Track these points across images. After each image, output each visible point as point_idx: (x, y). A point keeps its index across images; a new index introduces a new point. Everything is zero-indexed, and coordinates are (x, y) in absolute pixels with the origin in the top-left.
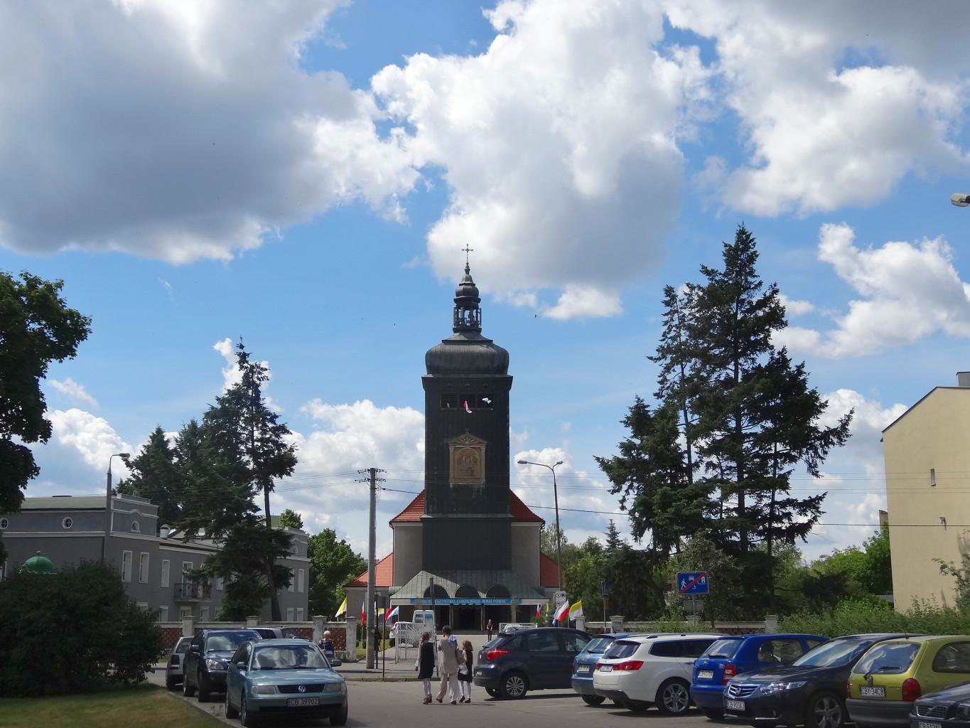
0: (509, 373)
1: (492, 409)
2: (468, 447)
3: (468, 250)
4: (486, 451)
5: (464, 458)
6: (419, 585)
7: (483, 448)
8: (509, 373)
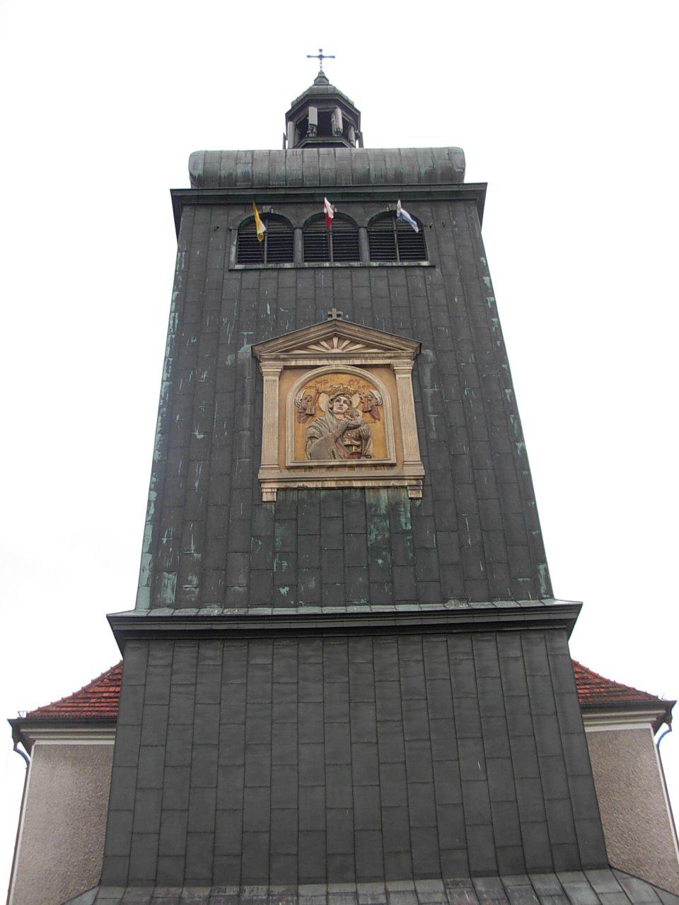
1: (425, 263)
3: (321, 57)
7: (404, 366)
8: (469, 178)
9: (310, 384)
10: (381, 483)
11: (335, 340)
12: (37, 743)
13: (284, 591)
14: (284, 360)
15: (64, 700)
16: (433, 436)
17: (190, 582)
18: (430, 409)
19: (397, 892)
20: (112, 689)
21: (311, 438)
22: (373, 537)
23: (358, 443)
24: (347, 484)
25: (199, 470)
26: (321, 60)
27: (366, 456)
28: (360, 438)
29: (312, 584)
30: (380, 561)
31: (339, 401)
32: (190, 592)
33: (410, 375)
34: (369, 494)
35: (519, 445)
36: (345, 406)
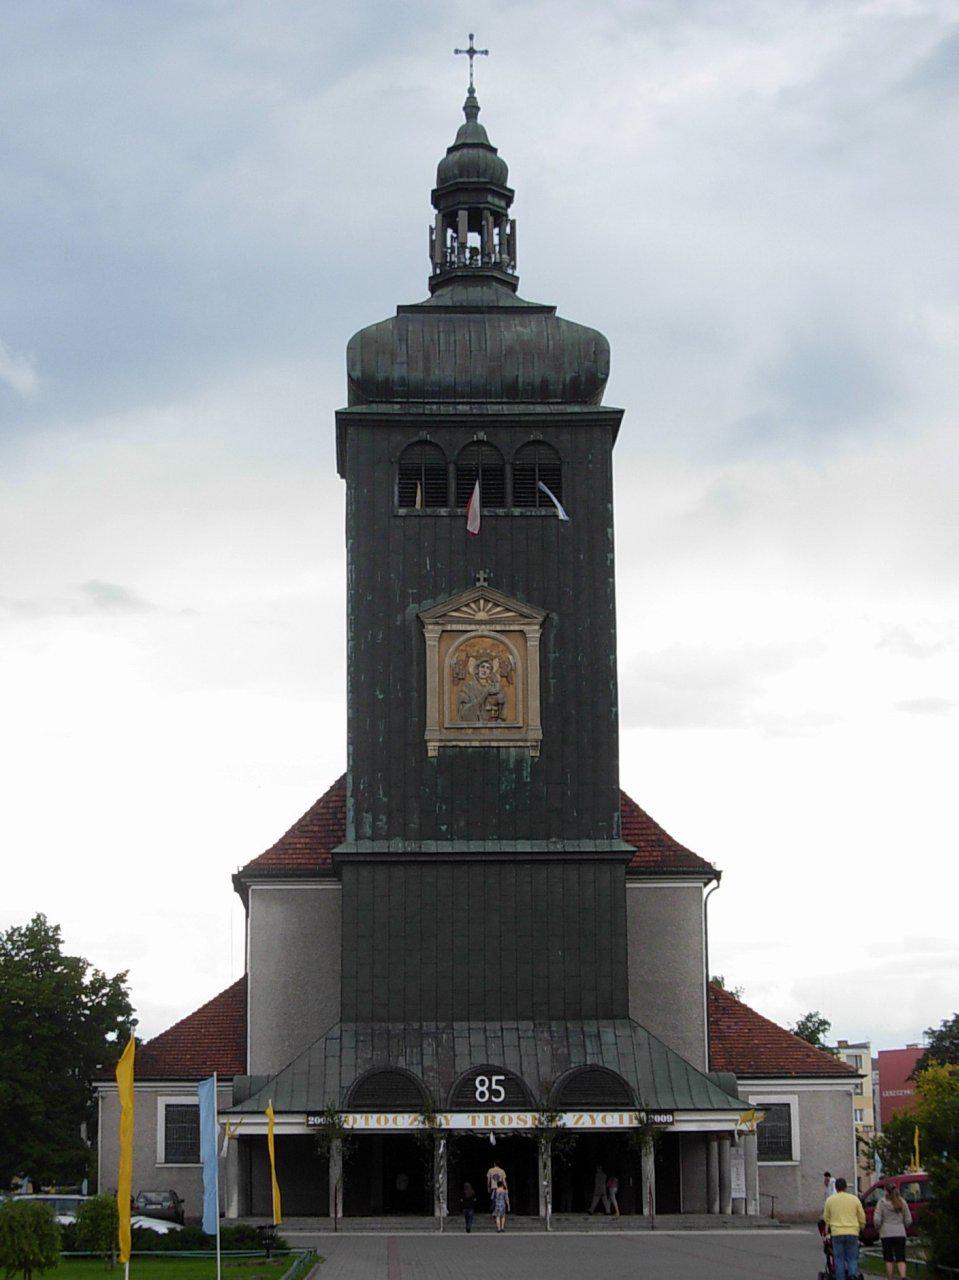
0: (609, 400)
2: (484, 629)
3: (471, 52)
4: (543, 641)
5: (472, 662)
6: (333, 1062)
7: (534, 631)
8: (609, 400)
9: (461, 647)
10: (511, 744)
11: (482, 602)
12: (253, 887)
13: (444, 828)
14: (442, 624)
15: (268, 852)
16: (551, 700)
17: (381, 820)
18: (551, 674)
19: (507, 1029)
20: (302, 840)
21: (463, 702)
22: (504, 786)
23: (496, 708)
24: (487, 744)
25: (382, 728)
26: (471, 57)
27: (504, 720)
28: (497, 704)
29: (462, 824)
30: (508, 807)
31: (483, 667)
32: (382, 828)
33: (537, 643)
34: (503, 751)
35: (614, 710)
36: (488, 671)
